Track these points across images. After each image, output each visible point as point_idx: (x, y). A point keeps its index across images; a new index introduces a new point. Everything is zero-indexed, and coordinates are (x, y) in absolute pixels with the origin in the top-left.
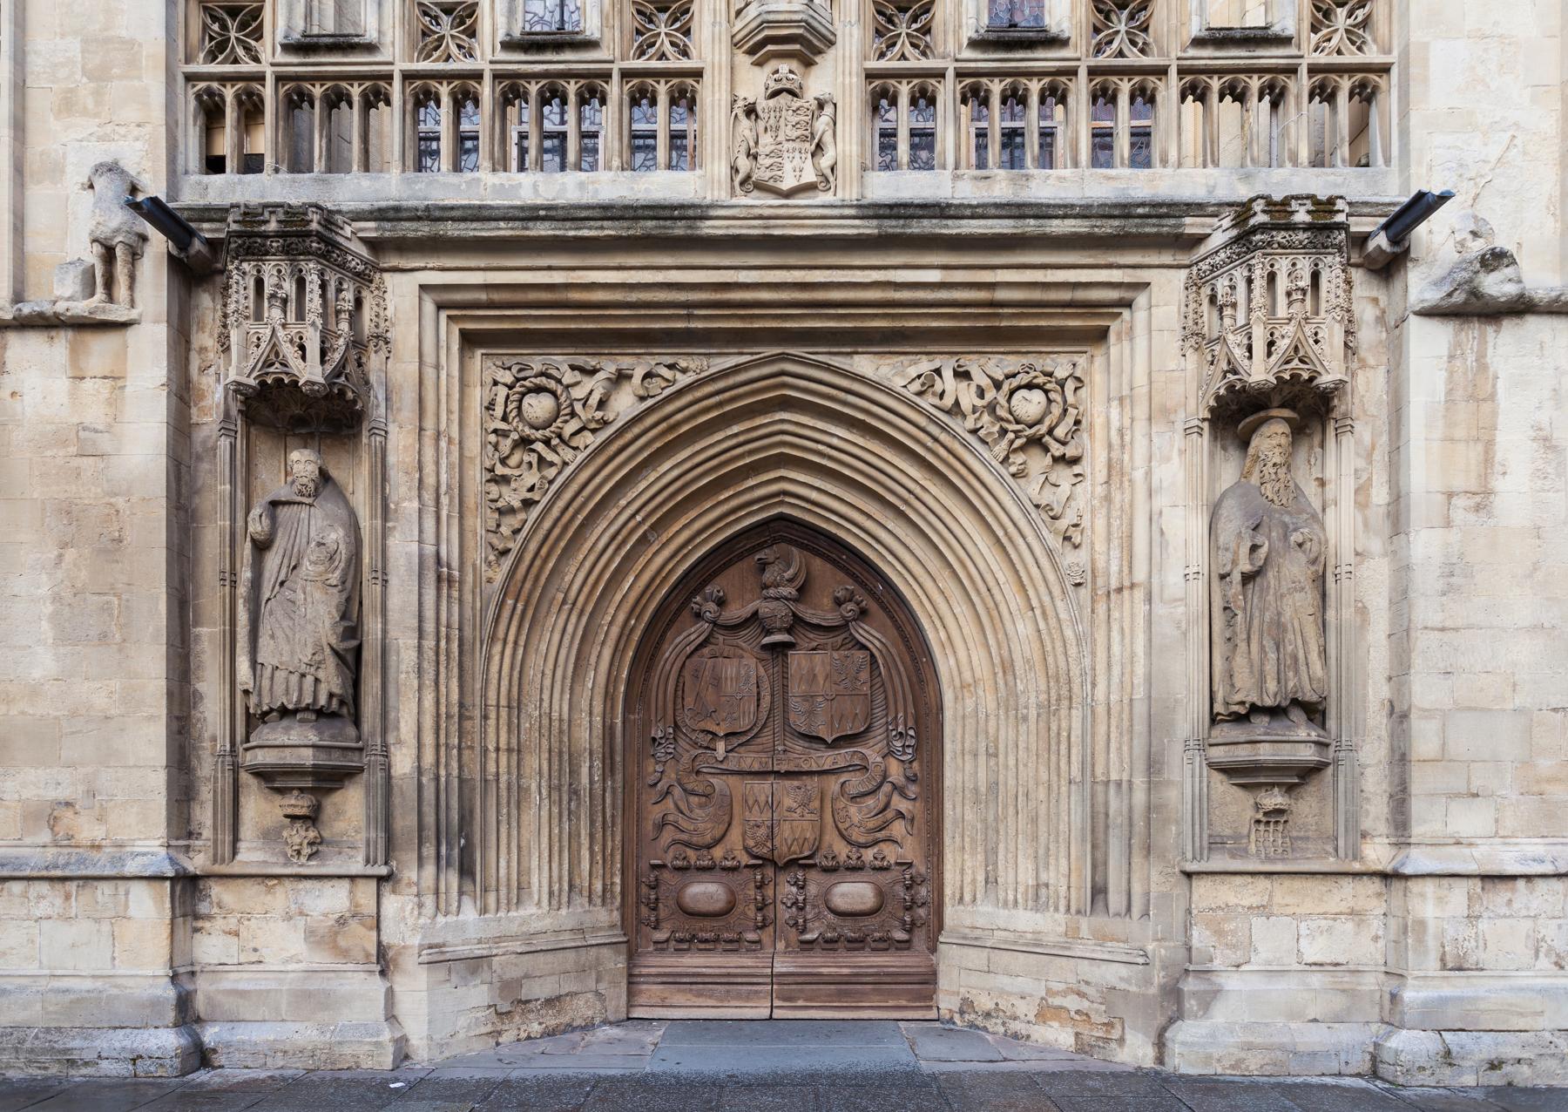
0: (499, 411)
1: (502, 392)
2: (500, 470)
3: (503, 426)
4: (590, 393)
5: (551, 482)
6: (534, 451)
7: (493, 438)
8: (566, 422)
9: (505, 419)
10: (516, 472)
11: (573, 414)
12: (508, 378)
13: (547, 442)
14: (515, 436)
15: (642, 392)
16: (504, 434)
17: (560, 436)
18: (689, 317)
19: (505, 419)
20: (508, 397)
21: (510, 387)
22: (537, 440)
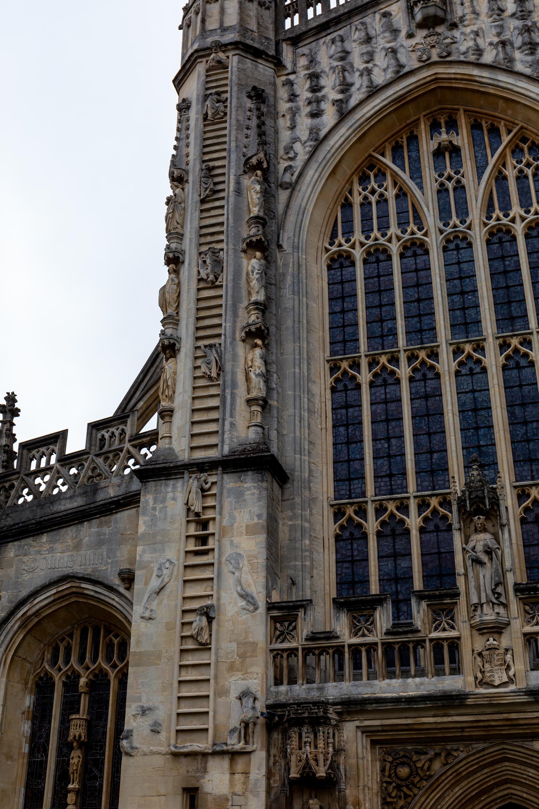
0: (387, 773)
1: (388, 765)
2: (389, 800)
3: (388, 780)
4: (424, 765)
5: (409, 804)
6: (403, 791)
7: (385, 785)
8: (415, 777)
9: (390, 776)
10: (395, 800)
11: (418, 774)
12: (390, 759)
13: (407, 786)
14: (394, 784)
15: (445, 762)
16: (389, 783)
17: (413, 783)
18: (462, 732)
19: (390, 776)
20: (390, 767)
21: (391, 763)
22: (403, 786)
